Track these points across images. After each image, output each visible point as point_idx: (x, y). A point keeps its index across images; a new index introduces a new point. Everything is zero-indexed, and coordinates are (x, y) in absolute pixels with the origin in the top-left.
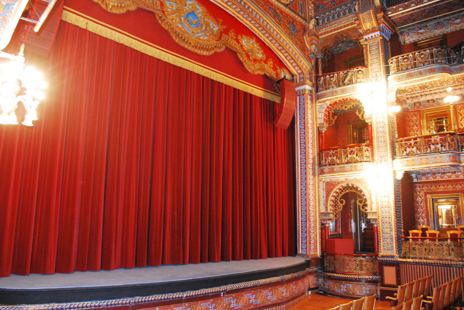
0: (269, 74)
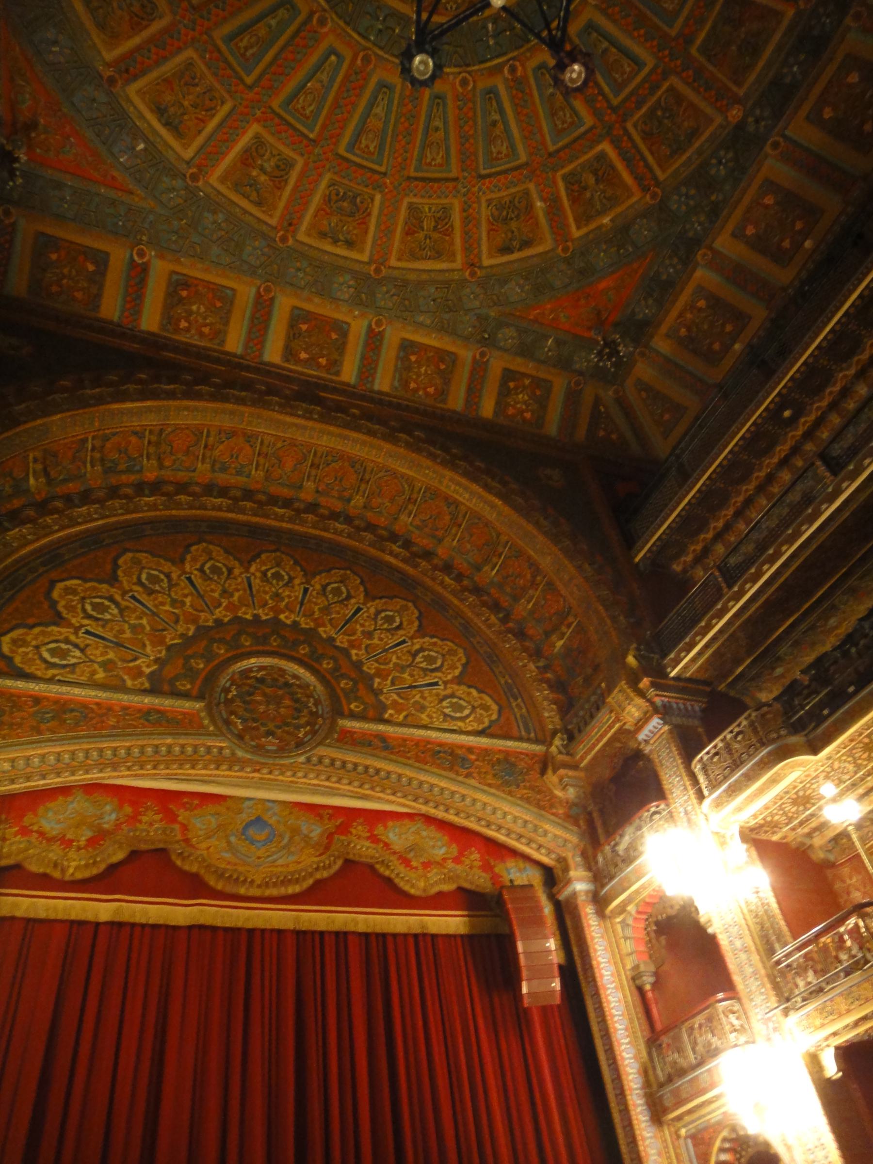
0: (471, 883)
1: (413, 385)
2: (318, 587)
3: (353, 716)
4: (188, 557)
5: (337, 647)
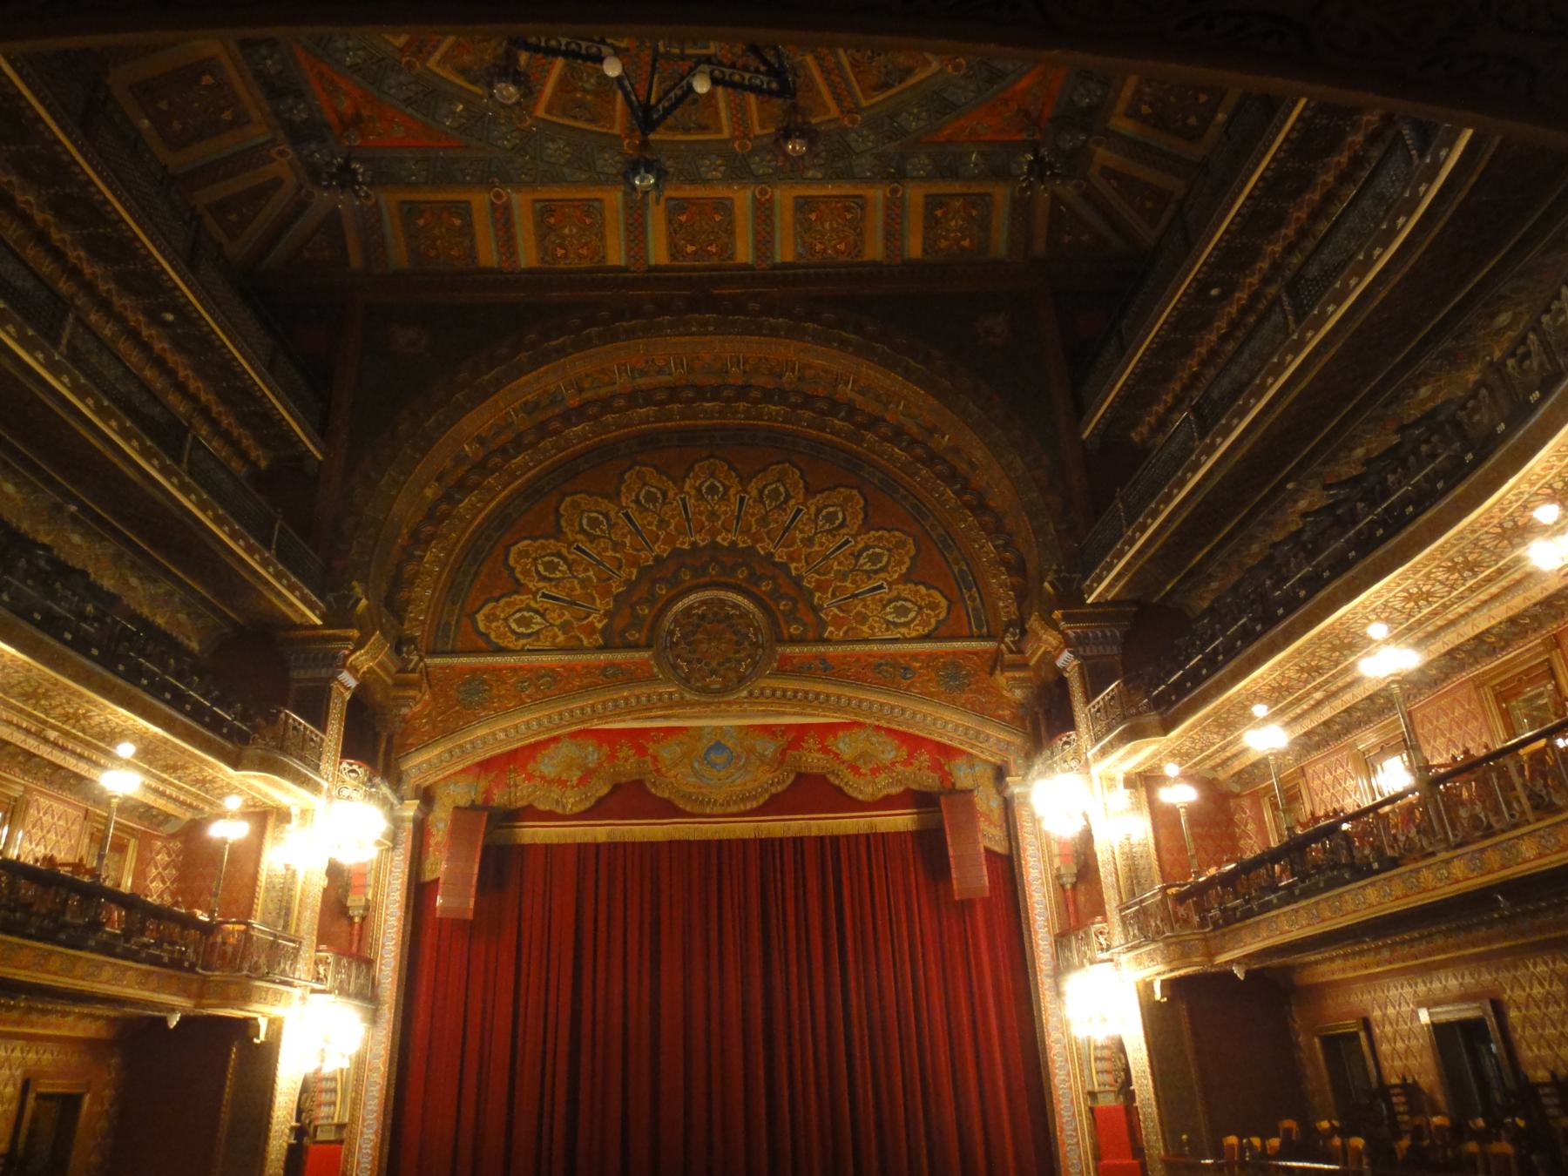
1: (818, 247)
2: (755, 493)
3: (793, 641)
4: (623, 489)
5: (775, 564)
